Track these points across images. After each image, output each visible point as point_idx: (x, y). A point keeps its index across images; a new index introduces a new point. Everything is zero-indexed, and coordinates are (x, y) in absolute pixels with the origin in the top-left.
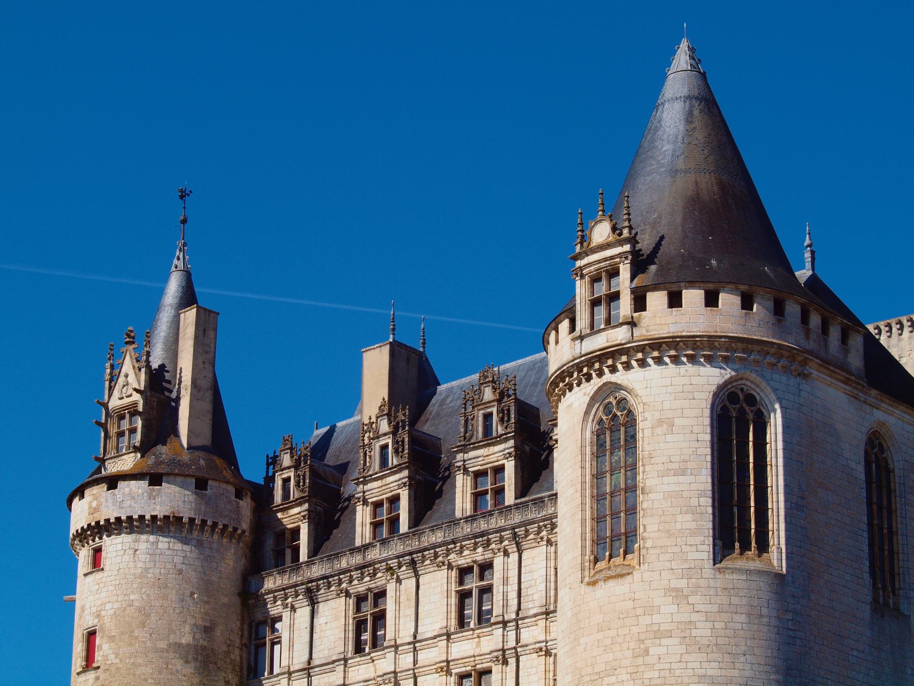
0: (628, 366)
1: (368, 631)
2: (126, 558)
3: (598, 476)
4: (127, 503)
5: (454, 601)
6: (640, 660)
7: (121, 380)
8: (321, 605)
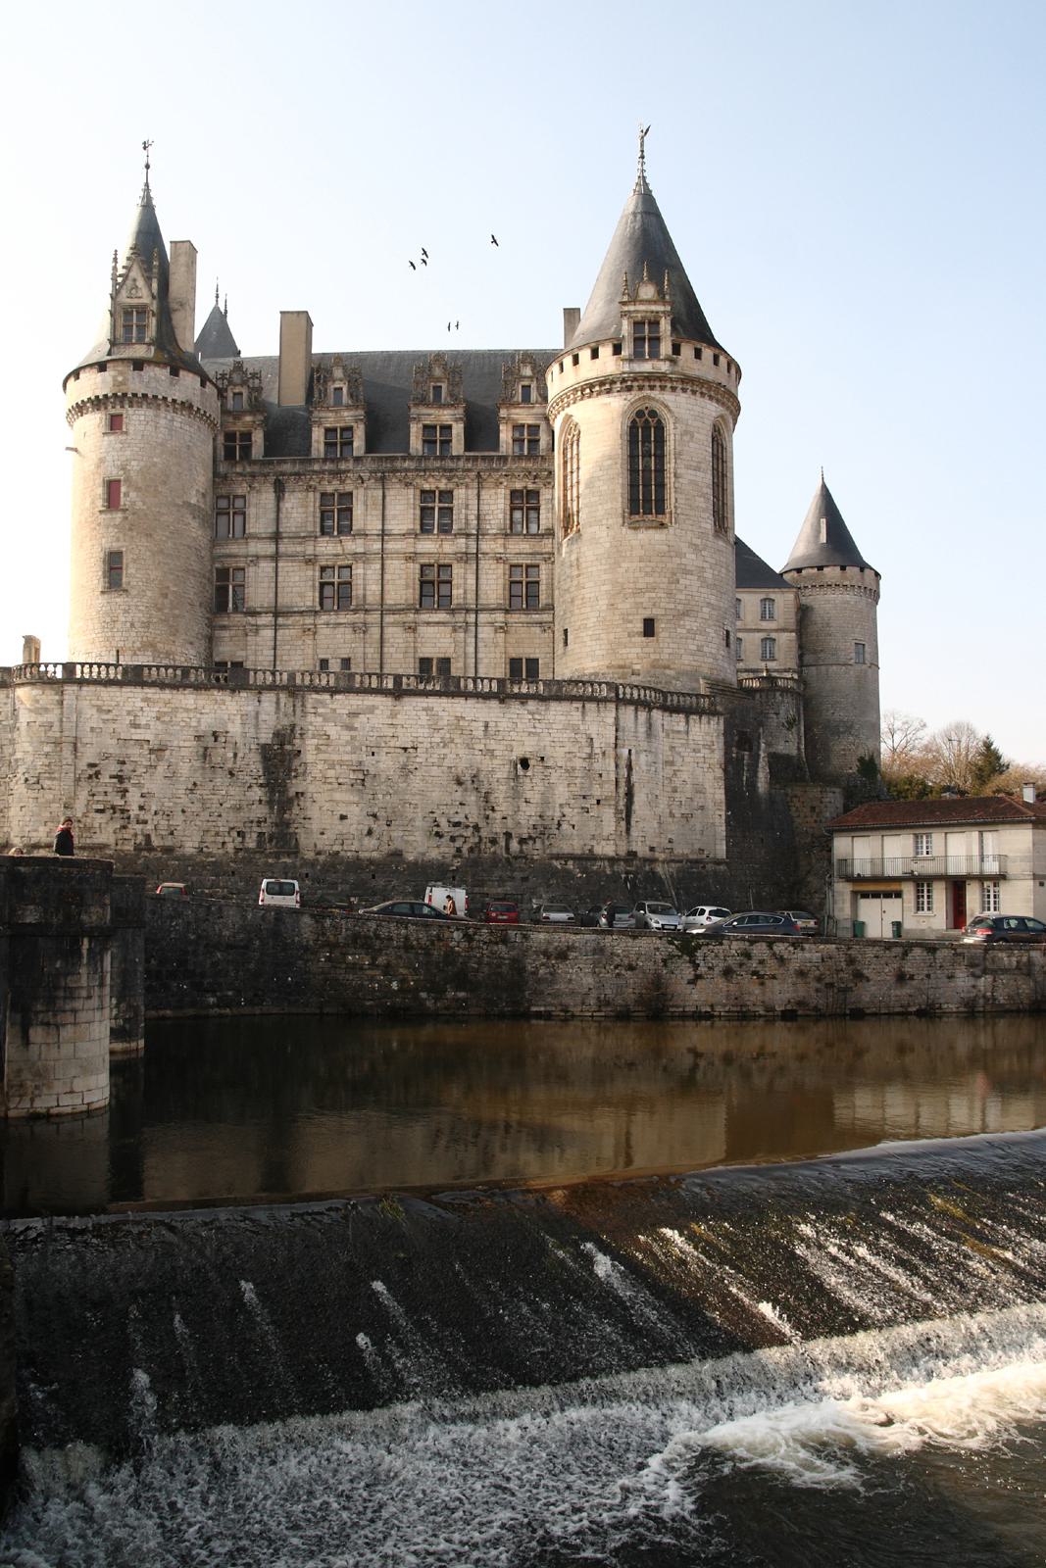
0: (663, 388)
1: (336, 516)
2: (149, 428)
4: (153, 385)
5: (418, 512)
8: (286, 495)
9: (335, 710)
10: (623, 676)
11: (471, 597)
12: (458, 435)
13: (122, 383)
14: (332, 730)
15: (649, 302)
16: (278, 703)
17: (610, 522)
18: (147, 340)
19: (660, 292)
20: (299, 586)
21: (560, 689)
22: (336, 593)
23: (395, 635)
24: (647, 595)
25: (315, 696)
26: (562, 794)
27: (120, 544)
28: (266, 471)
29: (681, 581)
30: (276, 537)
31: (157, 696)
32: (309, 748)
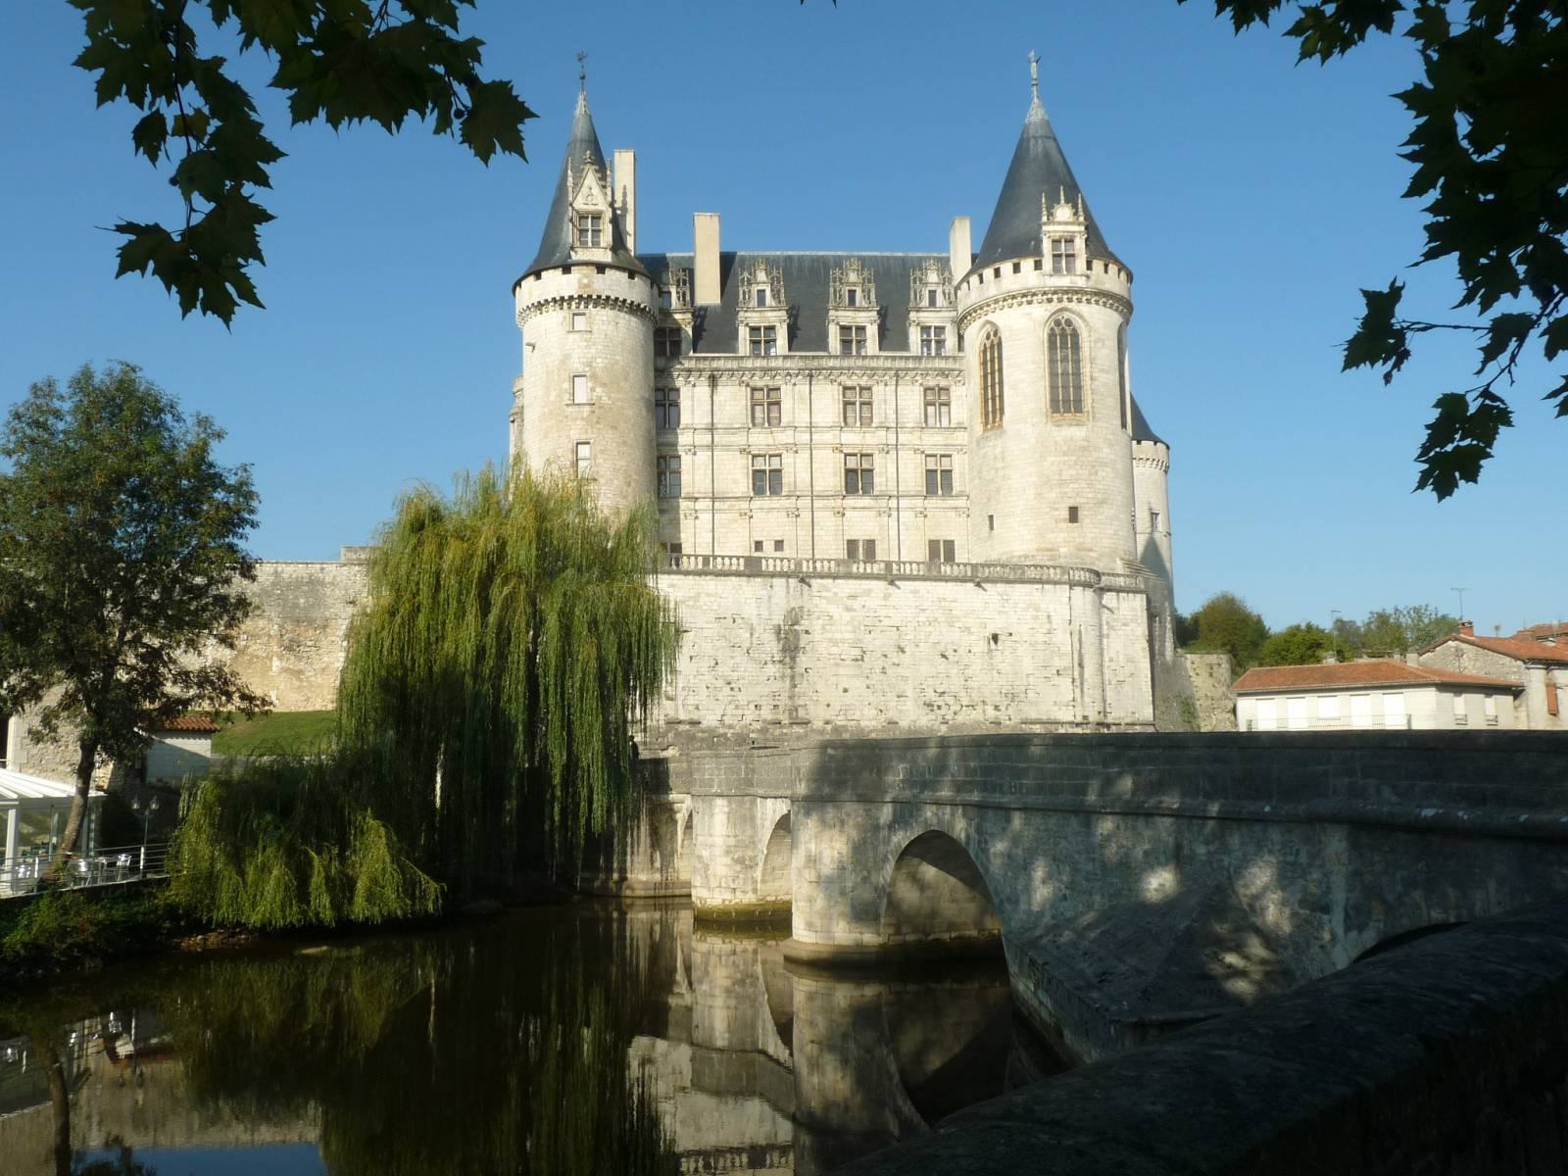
0: (1079, 301)
3: (1052, 361)
5: (841, 406)
6: (1093, 478)
7: (585, 190)
8: (719, 388)
9: (836, 594)
10: (1053, 558)
11: (892, 485)
12: (873, 336)
13: (587, 286)
14: (835, 611)
15: (1067, 223)
16: (788, 587)
17: (1034, 420)
18: (602, 244)
19: (1076, 214)
20: (736, 476)
21: (1023, 573)
22: (767, 481)
23: (826, 520)
24: (1071, 486)
25: (819, 581)
26: (1028, 665)
27: (588, 436)
28: (701, 366)
29: (1100, 473)
30: (711, 429)
31: (680, 582)
32: (816, 626)
